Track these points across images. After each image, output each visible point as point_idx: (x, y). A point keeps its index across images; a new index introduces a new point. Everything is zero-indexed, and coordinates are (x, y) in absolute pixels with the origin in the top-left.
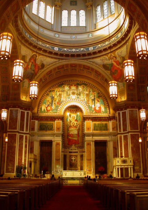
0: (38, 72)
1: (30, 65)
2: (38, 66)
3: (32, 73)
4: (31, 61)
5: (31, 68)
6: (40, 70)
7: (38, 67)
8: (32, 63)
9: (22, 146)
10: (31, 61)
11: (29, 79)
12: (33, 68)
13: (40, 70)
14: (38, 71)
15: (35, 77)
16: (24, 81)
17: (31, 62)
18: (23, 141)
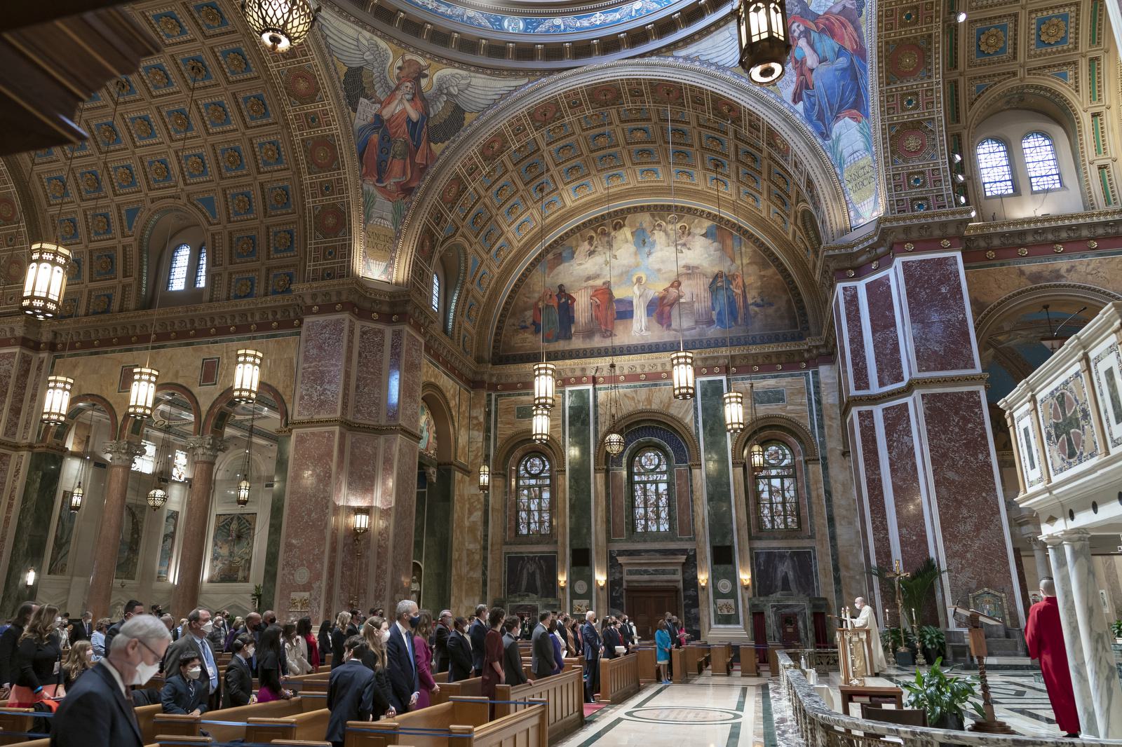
0: (860, 36)
1: (807, 51)
2: (839, 14)
3: (843, 70)
4: (796, 34)
5: (822, 60)
6: (862, 19)
7: (843, 19)
8: (806, 33)
9: (909, 467)
10: (796, 34)
11: (850, 108)
12: (828, 45)
13: (860, 14)
14: (857, 28)
15: (865, 68)
16: (834, 136)
17: (799, 38)
18: (908, 432)
